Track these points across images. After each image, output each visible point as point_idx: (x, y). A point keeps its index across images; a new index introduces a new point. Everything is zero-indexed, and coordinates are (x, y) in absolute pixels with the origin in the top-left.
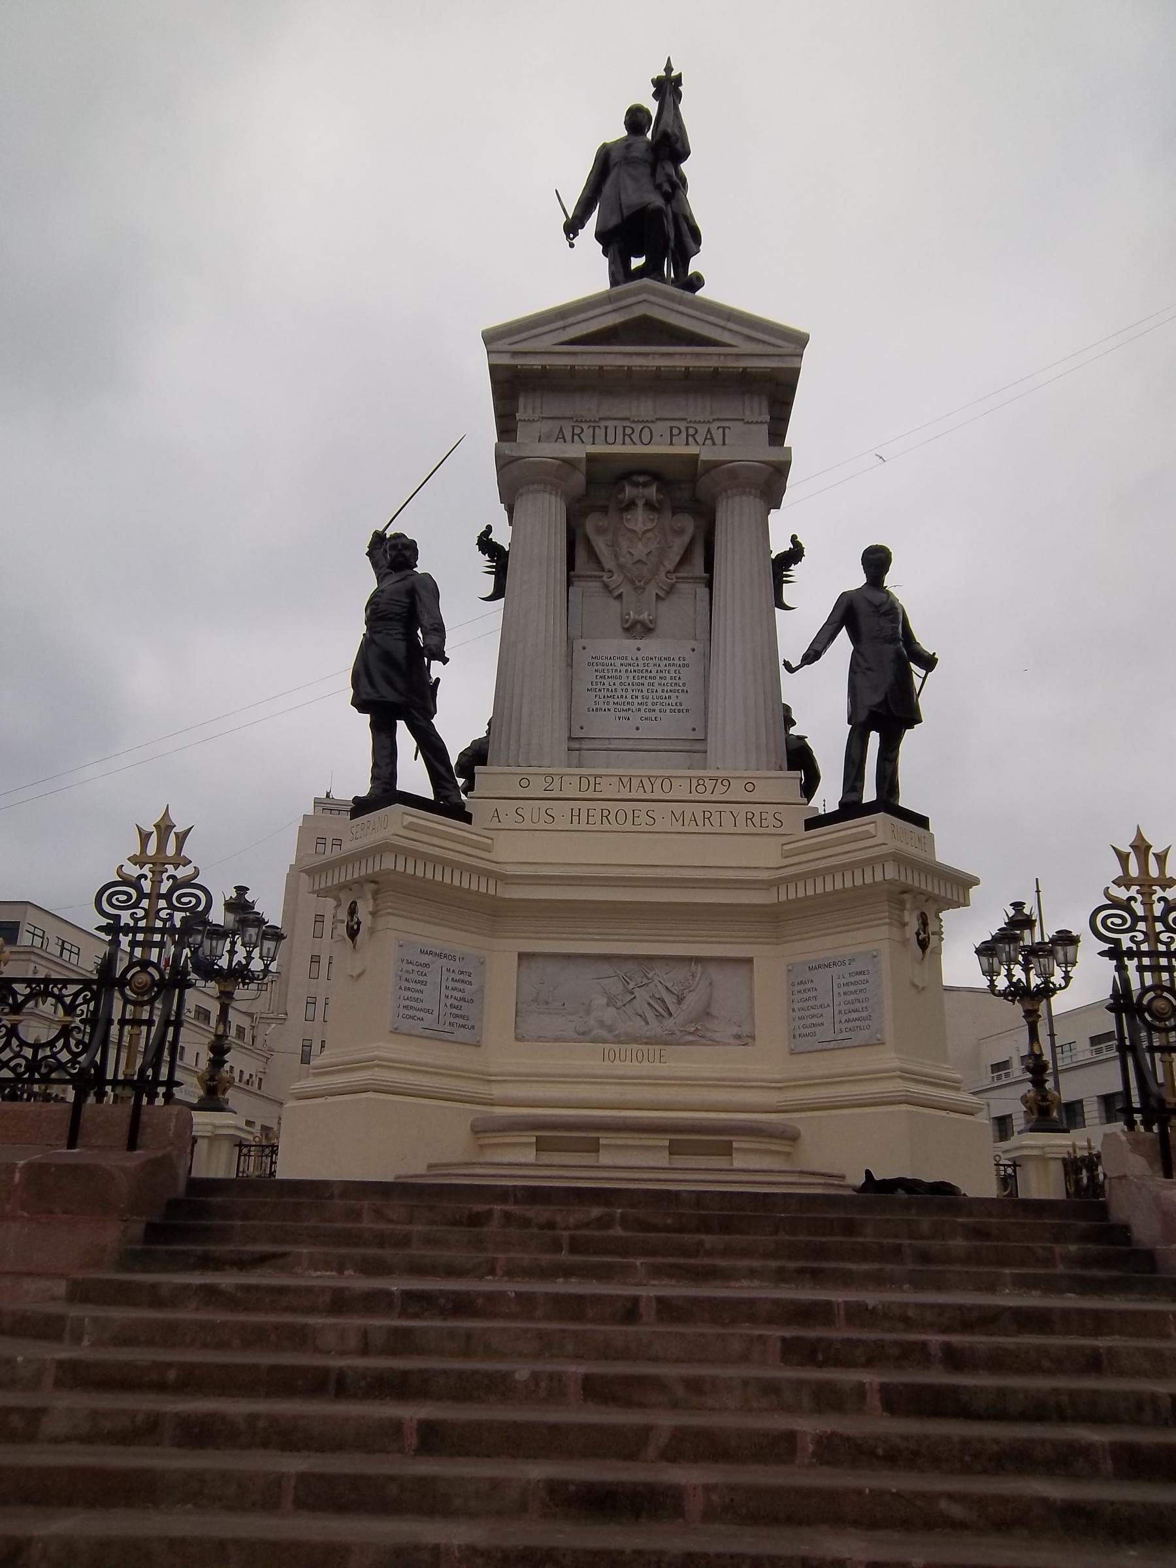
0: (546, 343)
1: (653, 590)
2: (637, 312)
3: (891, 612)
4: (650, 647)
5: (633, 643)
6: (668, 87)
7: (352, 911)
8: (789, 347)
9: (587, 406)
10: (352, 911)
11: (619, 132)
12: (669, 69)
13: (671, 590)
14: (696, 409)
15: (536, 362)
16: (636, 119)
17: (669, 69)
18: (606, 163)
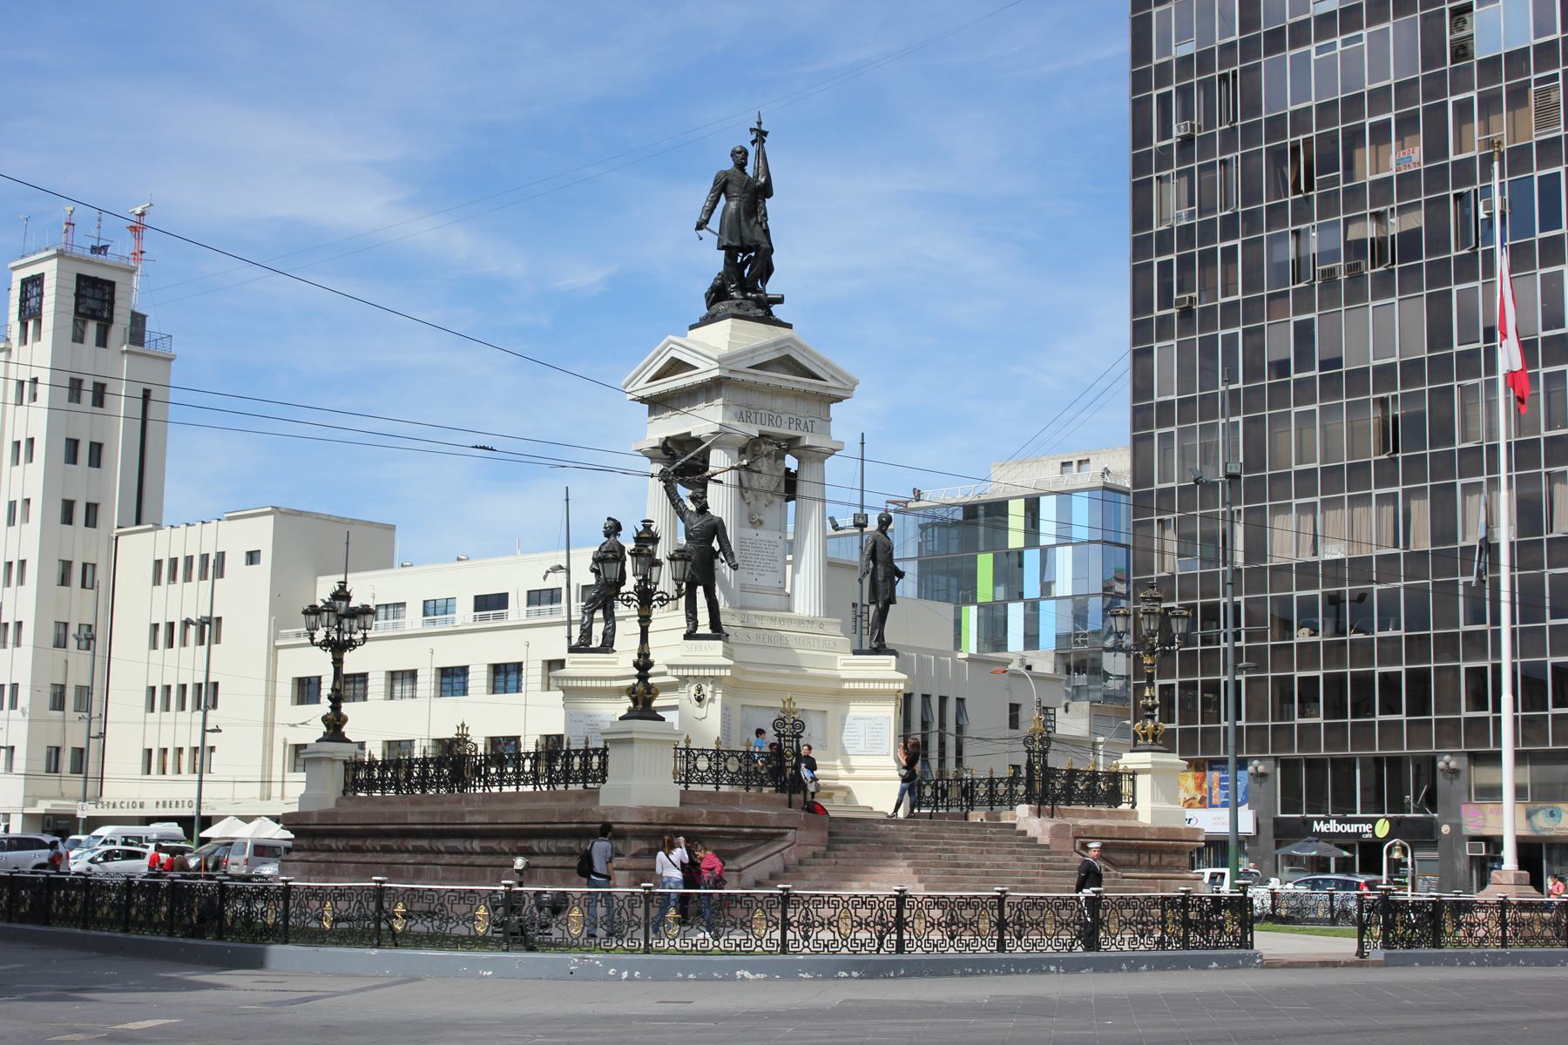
0: (742, 366)
1: (763, 501)
2: (785, 352)
3: (889, 550)
4: (763, 534)
5: (754, 532)
6: (760, 135)
7: (699, 690)
8: (849, 385)
9: (754, 399)
10: (699, 690)
11: (729, 165)
12: (760, 123)
13: (771, 502)
14: (801, 408)
15: (740, 377)
16: (740, 157)
17: (760, 123)
18: (722, 187)
